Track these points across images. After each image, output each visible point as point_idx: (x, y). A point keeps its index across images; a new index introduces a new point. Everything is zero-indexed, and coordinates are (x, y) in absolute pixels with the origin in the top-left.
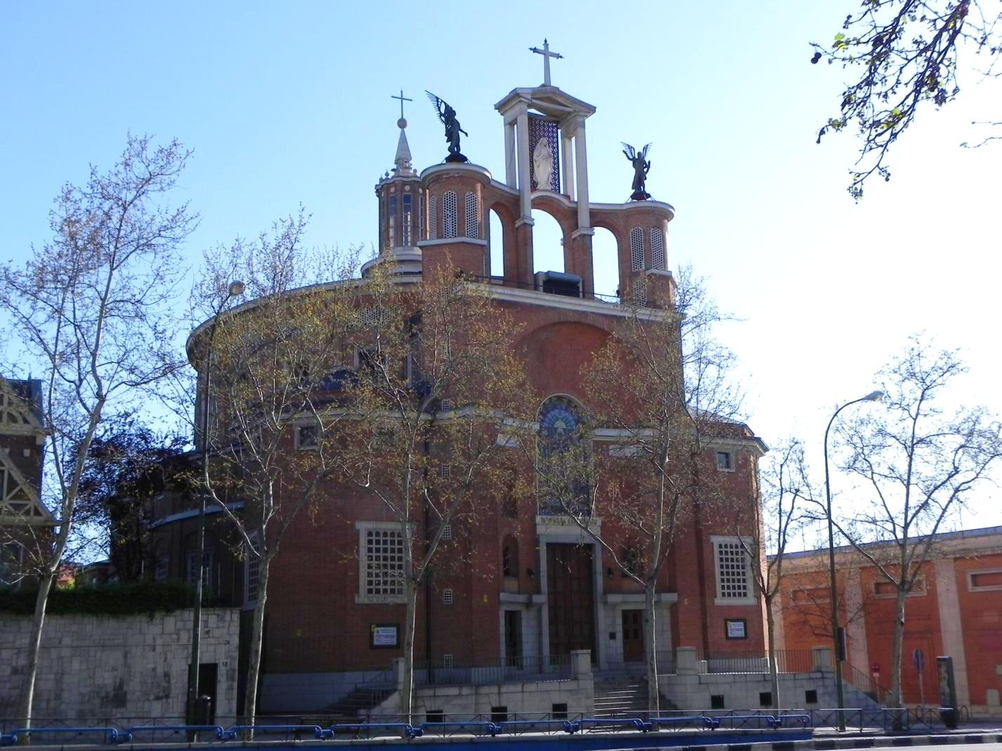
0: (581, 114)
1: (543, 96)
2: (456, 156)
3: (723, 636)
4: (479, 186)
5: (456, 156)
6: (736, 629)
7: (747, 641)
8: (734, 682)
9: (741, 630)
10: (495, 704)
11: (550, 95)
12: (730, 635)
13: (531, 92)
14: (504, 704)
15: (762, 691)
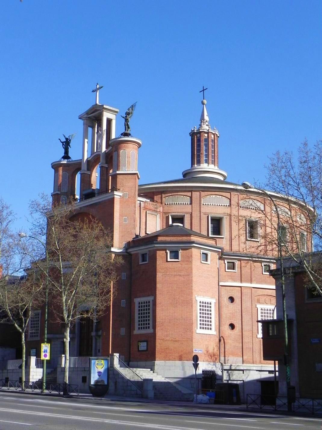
0: (102, 111)
1: (92, 111)
2: (66, 157)
3: (137, 349)
4: (61, 169)
5: (66, 157)
6: (143, 346)
7: (147, 352)
8: (73, 371)
9: (145, 346)
10: (6, 377)
11: (95, 109)
12: (140, 349)
13: (85, 113)
14: (8, 377)
15: (83, 375)
